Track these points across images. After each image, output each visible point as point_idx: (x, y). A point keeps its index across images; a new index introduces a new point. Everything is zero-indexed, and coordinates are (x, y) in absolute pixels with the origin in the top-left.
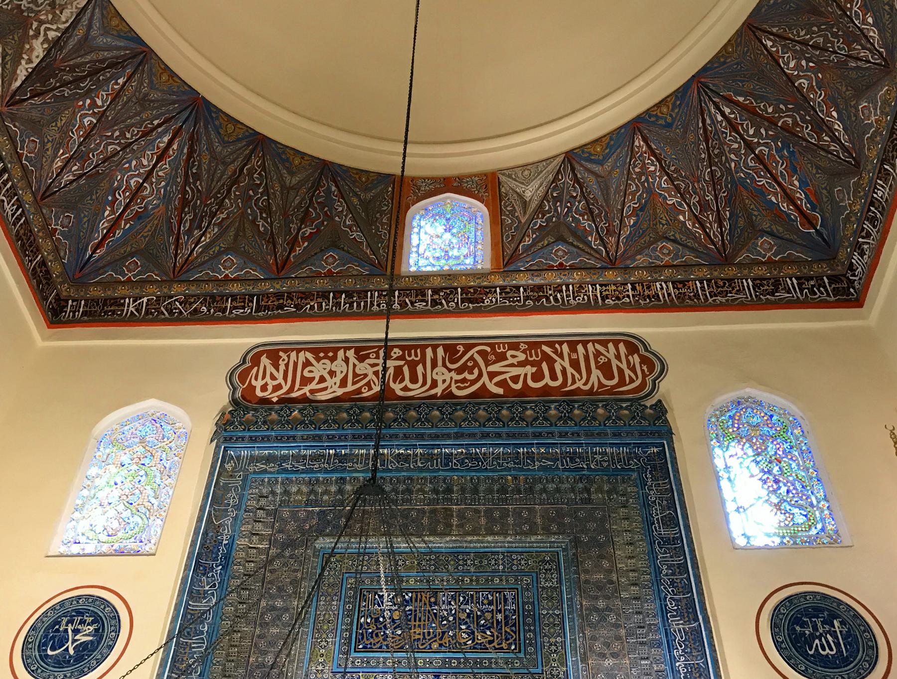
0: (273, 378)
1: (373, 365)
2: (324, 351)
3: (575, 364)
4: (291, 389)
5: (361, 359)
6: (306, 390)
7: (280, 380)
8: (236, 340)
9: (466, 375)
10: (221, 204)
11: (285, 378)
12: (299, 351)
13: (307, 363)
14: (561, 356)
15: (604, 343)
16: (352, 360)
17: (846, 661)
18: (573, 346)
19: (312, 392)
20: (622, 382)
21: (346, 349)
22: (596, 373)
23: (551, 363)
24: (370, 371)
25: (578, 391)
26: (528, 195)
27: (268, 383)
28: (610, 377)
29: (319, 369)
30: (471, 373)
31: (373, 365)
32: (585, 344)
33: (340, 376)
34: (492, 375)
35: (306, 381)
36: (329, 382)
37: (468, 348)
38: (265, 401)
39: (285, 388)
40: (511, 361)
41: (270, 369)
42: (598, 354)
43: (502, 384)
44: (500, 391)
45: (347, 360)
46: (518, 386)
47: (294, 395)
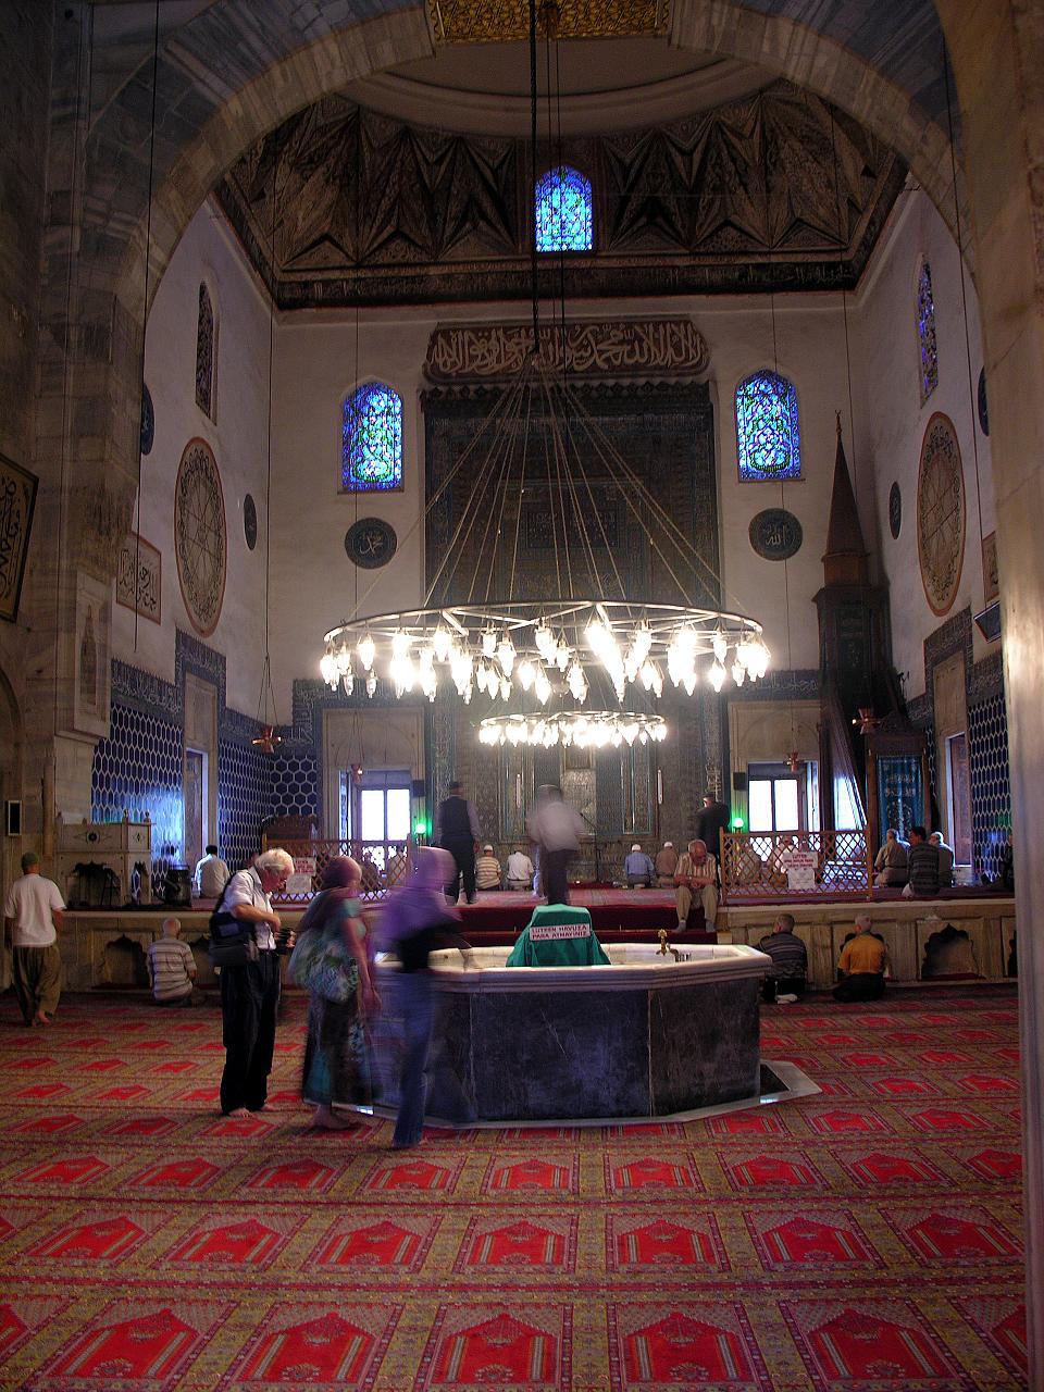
0: (450, 356)
1: (518, 344)
2: (482, 331)
3: (656, 341)
4: (463, 367)
5: (509, 338)
6: (474, 365)
7: (454, 358)
8: (420, 322)
9: (582, 352)
10: (383, 192)
11: (458, 356)
12: (463, 330)
13: (471, 343)
14: (648, 335)
15: (677, 323)
16: (502, 340)
17: (784, 548)
18: (656, 325)
19: (479, 367)
20: (687, 360)
21: (497, 329)
22: (671, 350)
23: (641, 340)
24: (516, 349)
25: (658, 367)
26: (628, 161)
27: (448, 360)
28: (679, 354)
29: (479, 349)
30: (586, 351)
31: (518, 344)
32: (664, 323)
33: (495, 354)
34: (601, 352)
35: (473, 358)
36: (489, 360)
37: (583, 327)
38: (448, 376)
39: (460, 365)
40: (614, 340)
41: (446, 347)
42: (673, 333)
43: (607, 360)
44: (606, 367)
45: (498, 340)
46: (617, 363)
47: (466, 370)
